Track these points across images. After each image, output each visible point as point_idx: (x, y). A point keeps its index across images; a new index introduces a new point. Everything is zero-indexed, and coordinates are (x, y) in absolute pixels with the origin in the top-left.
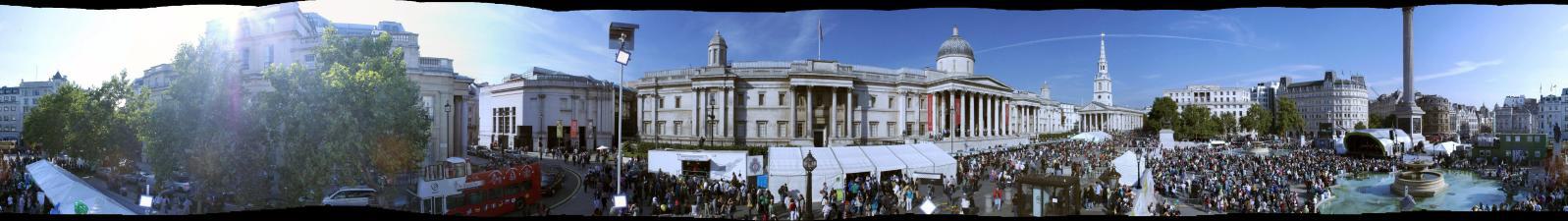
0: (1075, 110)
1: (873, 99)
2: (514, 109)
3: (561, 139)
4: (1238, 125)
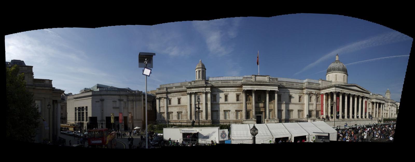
1: (290, 97)
2: (87, 107)
3: (113, 123)
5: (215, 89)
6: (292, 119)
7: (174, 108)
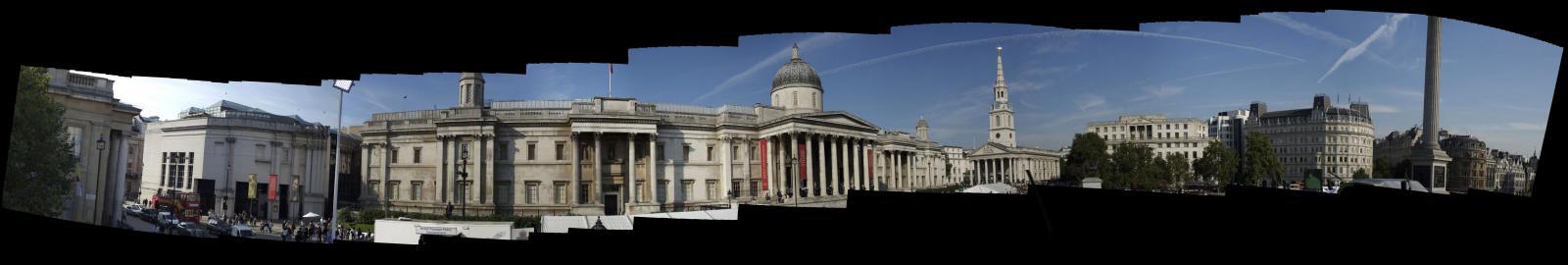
0: (965, 155)
1: (687, 148)
3: (254, 200)
4: (1191, 171)
5: (505, 129)
6: (693, 201)
7: (404, 171)
